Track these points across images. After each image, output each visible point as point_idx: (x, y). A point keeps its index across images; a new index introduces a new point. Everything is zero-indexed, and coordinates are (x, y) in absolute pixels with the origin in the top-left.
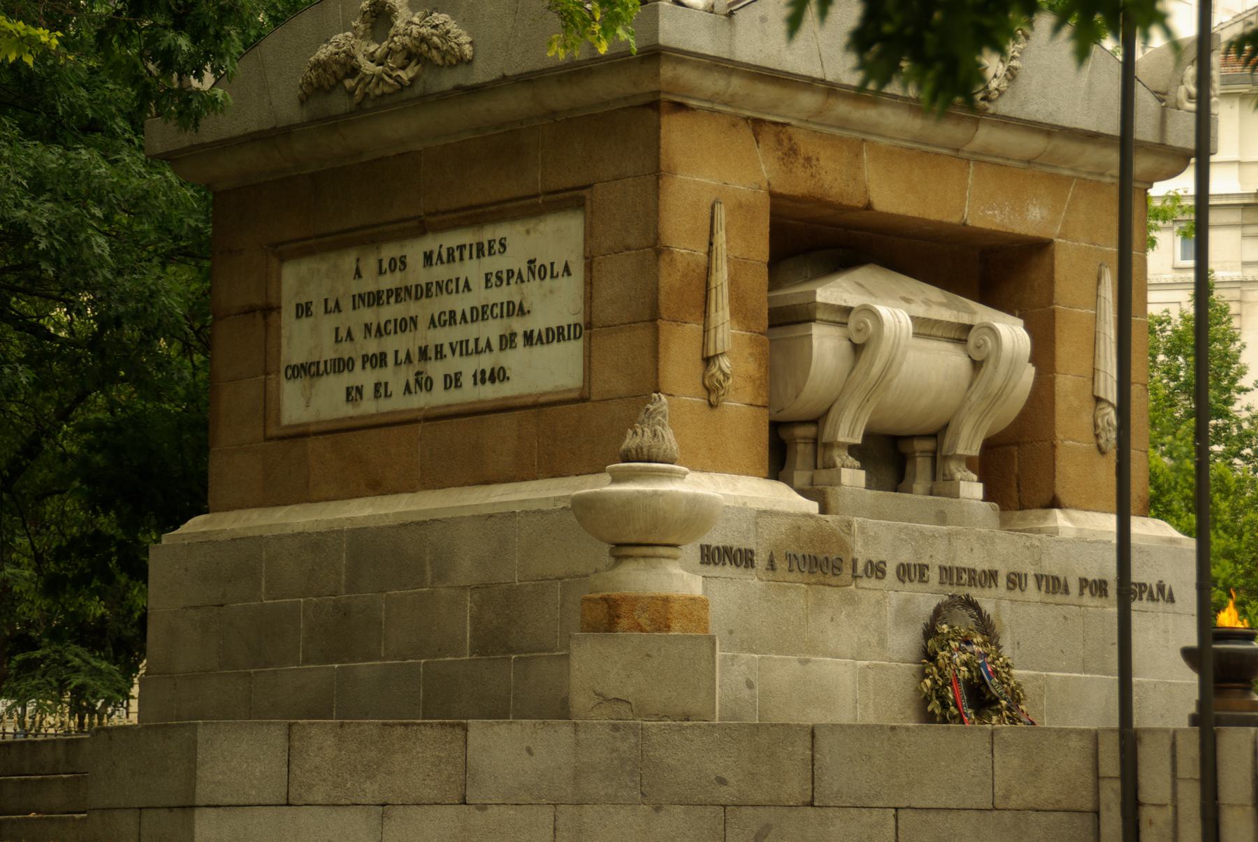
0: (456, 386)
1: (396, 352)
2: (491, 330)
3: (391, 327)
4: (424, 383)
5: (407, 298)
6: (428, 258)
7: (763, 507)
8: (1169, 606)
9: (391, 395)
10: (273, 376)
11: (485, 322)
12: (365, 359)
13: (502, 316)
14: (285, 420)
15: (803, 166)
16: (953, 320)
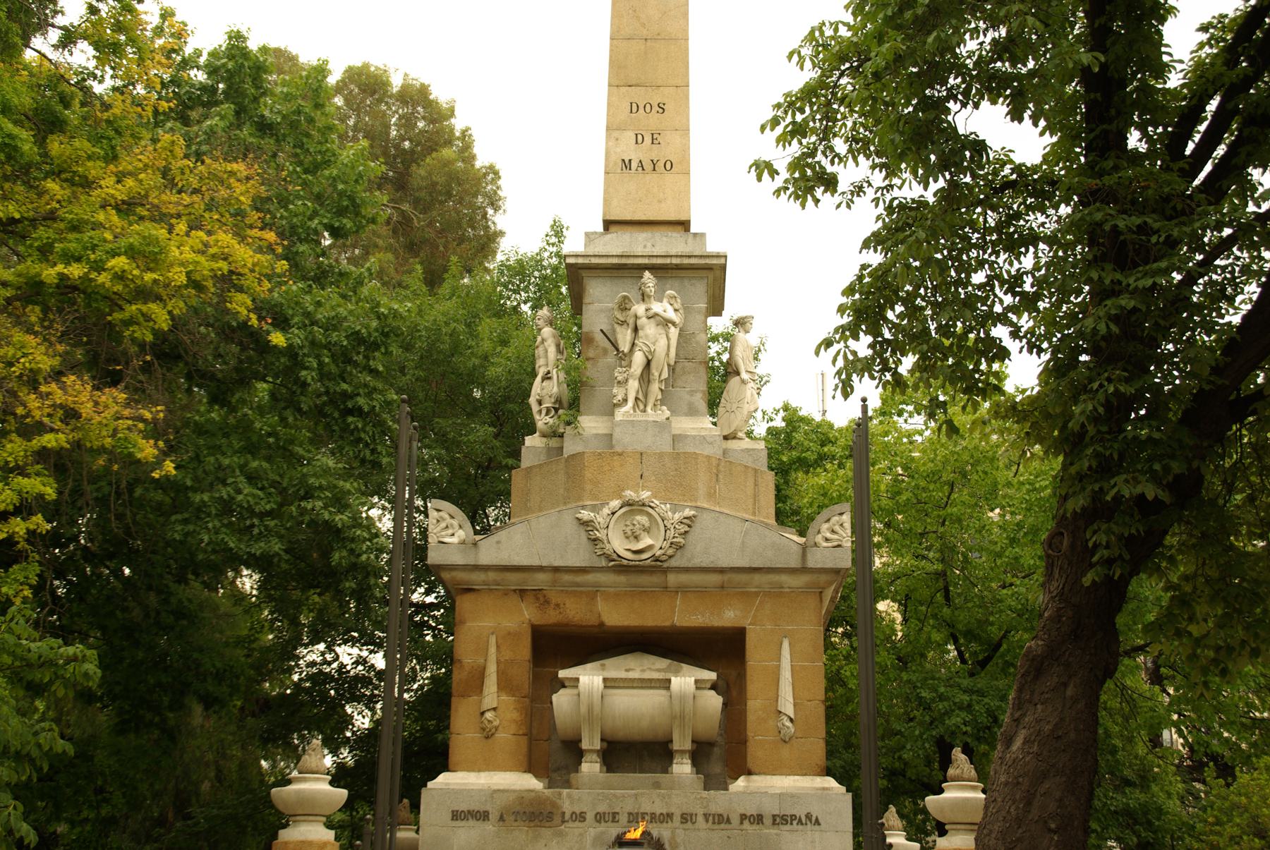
7: (495, 788)
8: (817, 827)
16: (661, 677)
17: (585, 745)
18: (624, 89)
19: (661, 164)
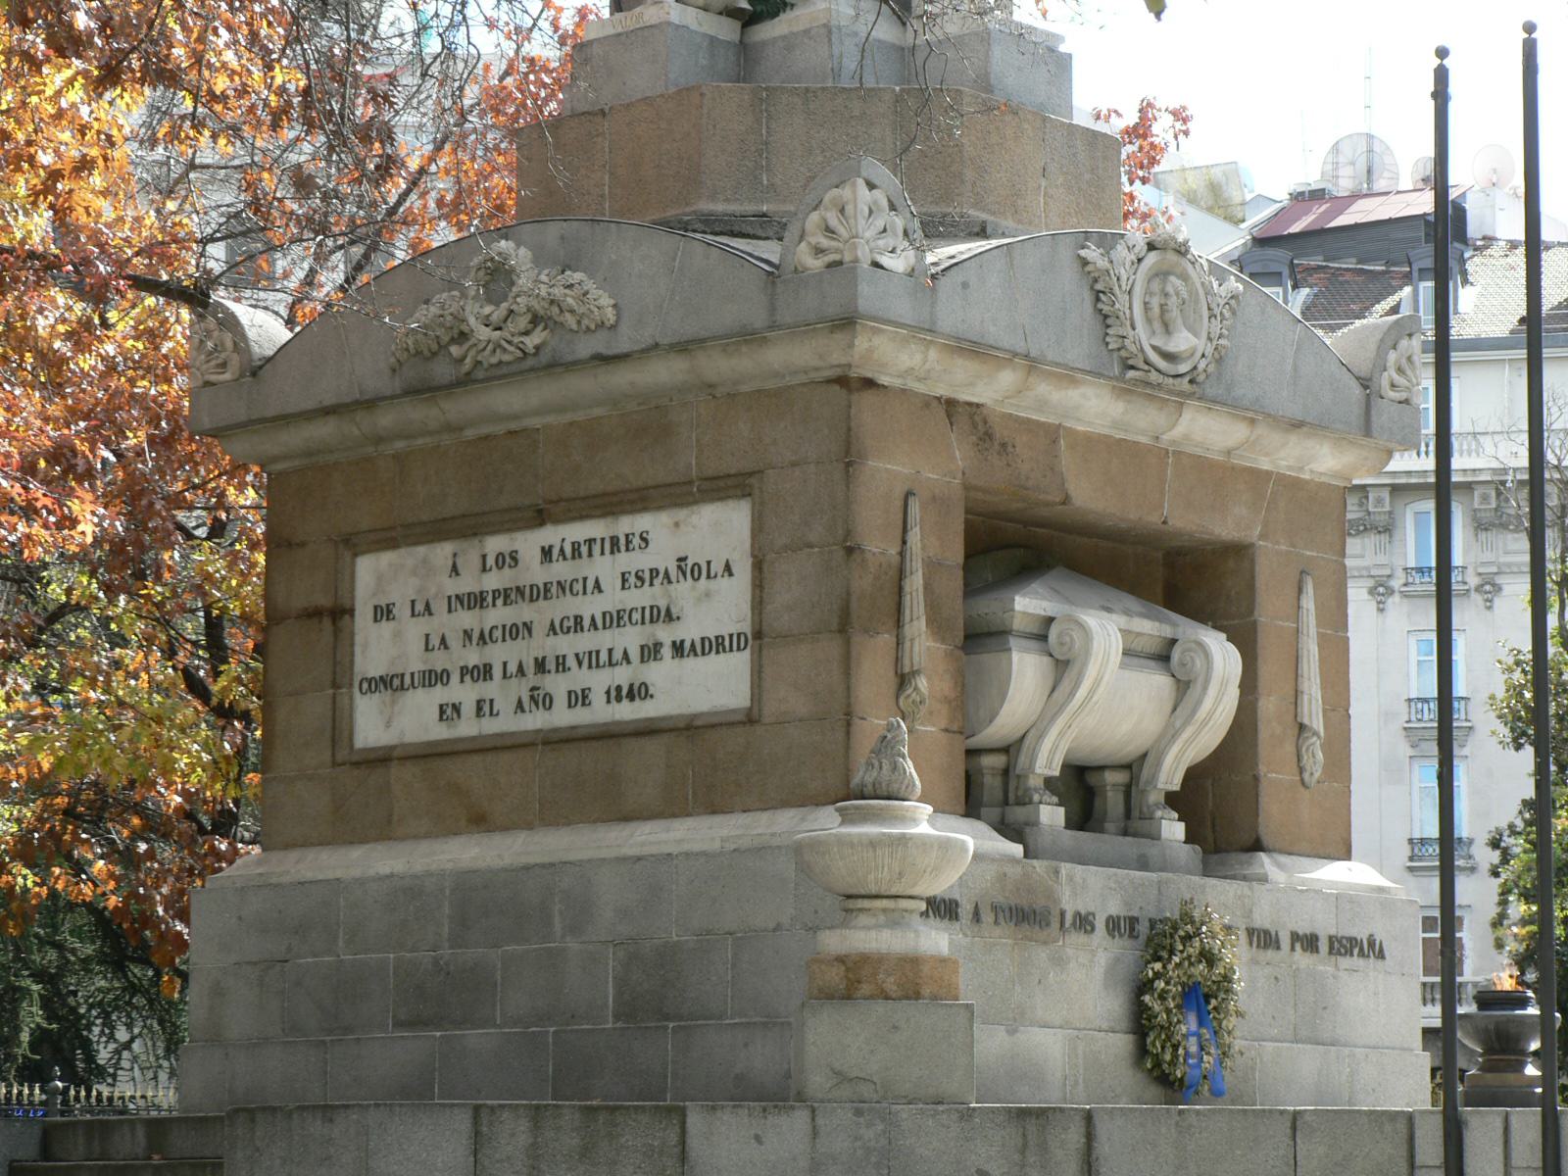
0: (583, 704)
1: (505, 664)
2: (630, 638)
3: (498, 634)
4: (544, 701)
5: (519, 599)
6: (546, 553)
8: (1380, 962)
9: (497, 714)
10: (344, 690)
11: (621, 629)
12: (464, 671)
13: (643, 623)
14: (359, 742)
15: (999, 453)
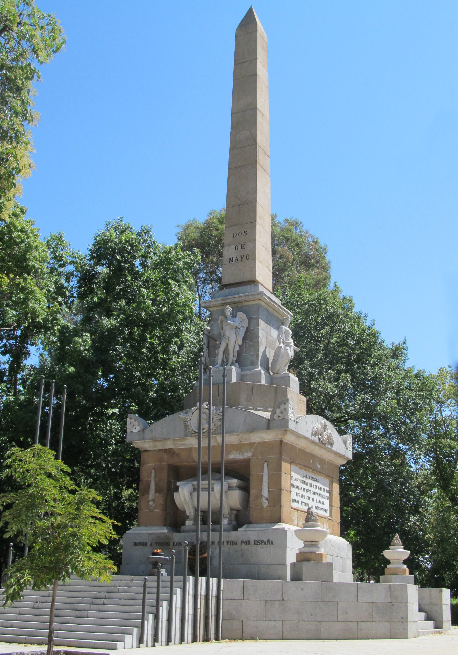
8: (272, 545)
17: (188, 514)
18: (231, 228)
19: (245, 257)
